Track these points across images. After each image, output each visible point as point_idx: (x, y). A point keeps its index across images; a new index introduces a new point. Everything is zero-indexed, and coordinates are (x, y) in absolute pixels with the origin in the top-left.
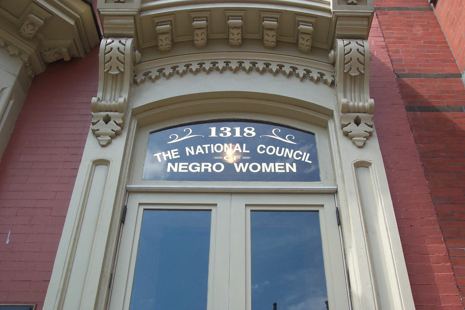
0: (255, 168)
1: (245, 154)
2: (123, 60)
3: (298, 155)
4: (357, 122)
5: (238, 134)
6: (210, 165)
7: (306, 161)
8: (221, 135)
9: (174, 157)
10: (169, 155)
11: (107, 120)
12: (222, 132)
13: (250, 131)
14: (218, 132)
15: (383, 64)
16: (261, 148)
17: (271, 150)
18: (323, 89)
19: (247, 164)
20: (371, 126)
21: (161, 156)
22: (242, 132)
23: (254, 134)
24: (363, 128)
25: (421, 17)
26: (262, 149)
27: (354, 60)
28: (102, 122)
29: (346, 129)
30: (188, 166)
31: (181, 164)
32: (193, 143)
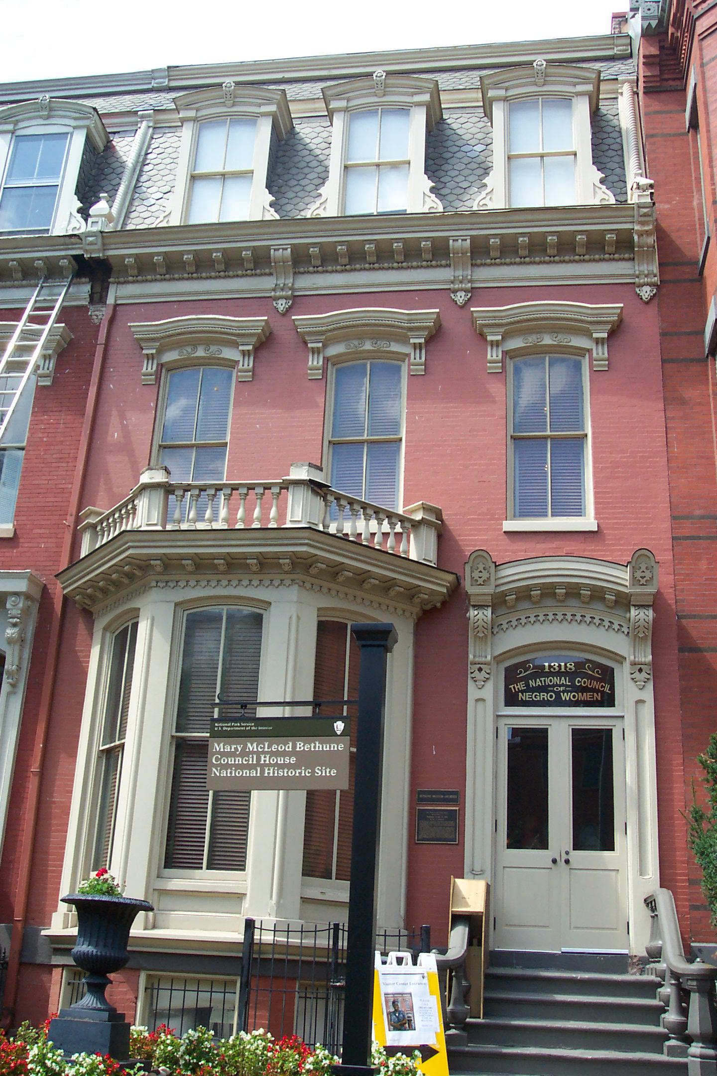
1: (567, 686)
2: (486, 627)
3: (602, 686)
4: (640, 670)
6: (546, 694)
7: (607, 691)
8: (552, 670)
9: (523, 688)
10: (519, 686)
11: (480, 670)
15: (670, 605)
16: (579, 680)
17: (585, 682)
18: (622, 637)
19: (569, 694)
20: (649, 674)
21: (514, 687)
23: (574, 669)
24: (644, 675)
26: (579, 682)
27: (642, 626)
28: (477, 671)
29: (633, 676)
30: (532, 695)
31: (527, 694)
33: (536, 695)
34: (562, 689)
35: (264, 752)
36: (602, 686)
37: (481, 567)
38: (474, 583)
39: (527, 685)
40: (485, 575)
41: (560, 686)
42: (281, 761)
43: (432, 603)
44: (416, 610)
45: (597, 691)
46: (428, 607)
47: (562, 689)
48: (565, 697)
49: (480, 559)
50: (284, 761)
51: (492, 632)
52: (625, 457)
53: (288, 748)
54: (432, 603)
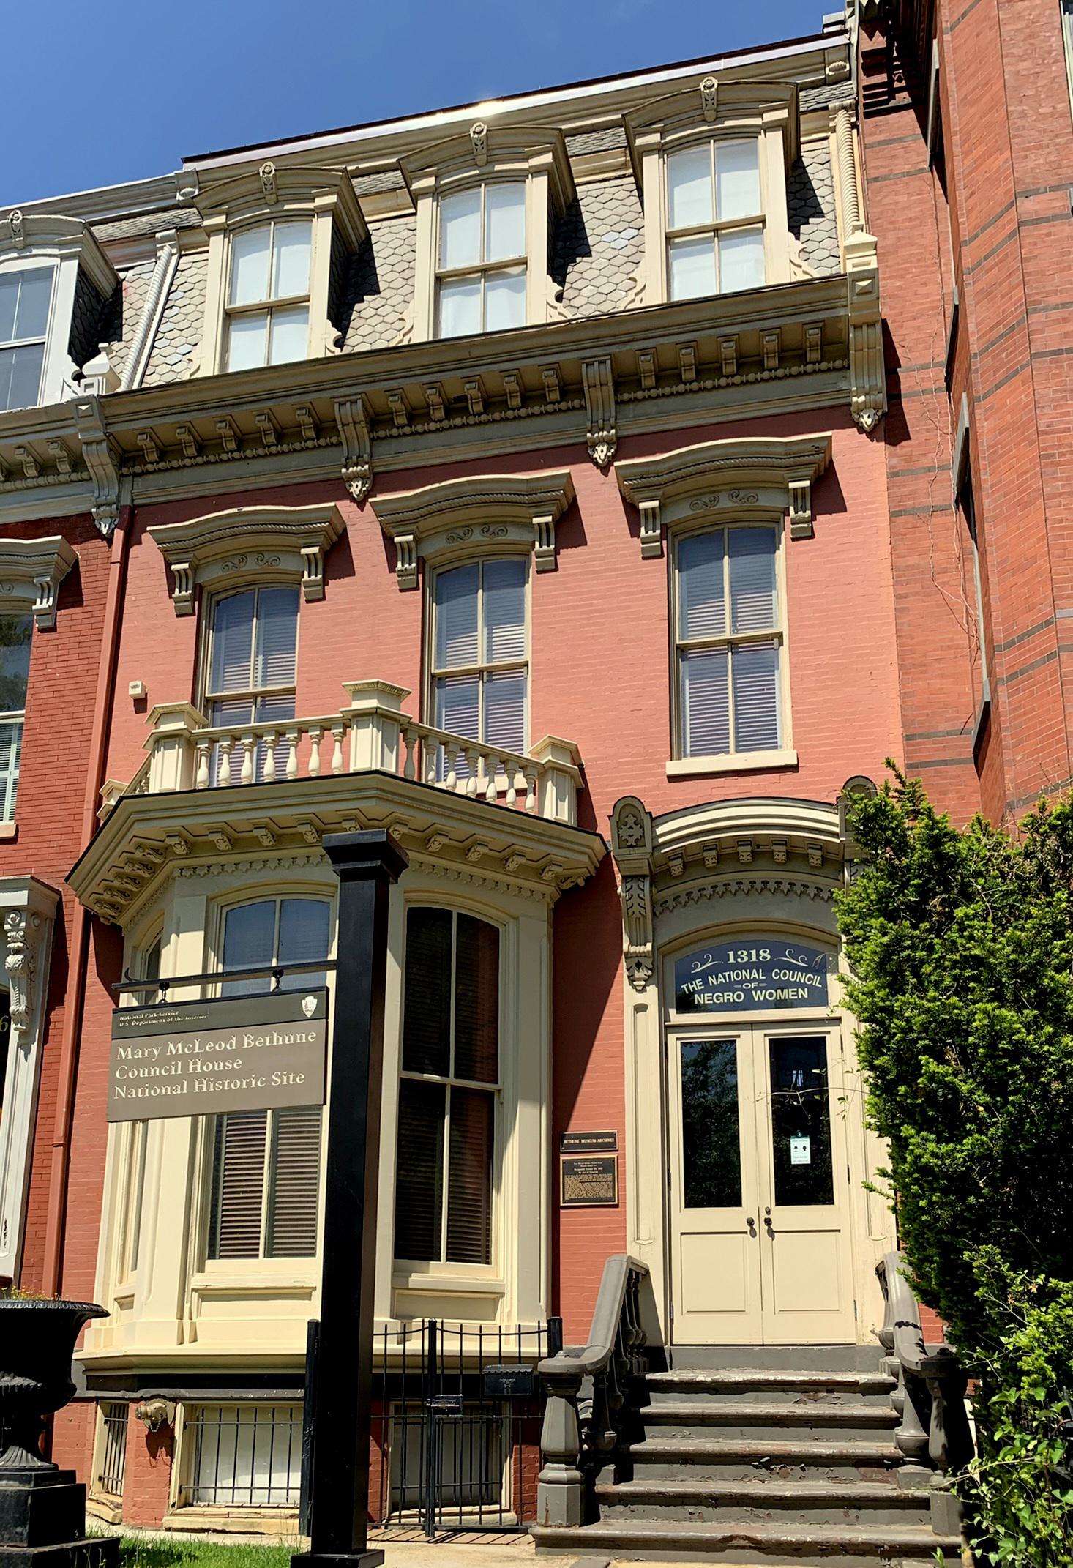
0: (771, 995)
1: (762, 981)
5: (754, 959)
8: (739, 960)
12: (739, 956)
13: (766, 955)
14: (736, 957)
21: (688, 987)
22: (758, 955)
23: (769, 957)
25: (959, 776)
26: (776, 973)
32: (714, 971)
33: (717, 997)
34: (753, 985)
35: (194, 1056)
36: (810, 979)
37: (631, 820)
38: (623, 844)
39: (705, 982)
40: (637, 832)
41: (751, 981)
42: (219, 1067)
43: (572, 879)
44: (549, 890)
45: (802, 986)
46: (567, 886)
47: (753, 985)
48: (758, 996)
49: (629, 809)
50: (224, 1066)
51: (654, 914)
52: (836, 658)
53: (231, 1046)
54: (572, 879)
